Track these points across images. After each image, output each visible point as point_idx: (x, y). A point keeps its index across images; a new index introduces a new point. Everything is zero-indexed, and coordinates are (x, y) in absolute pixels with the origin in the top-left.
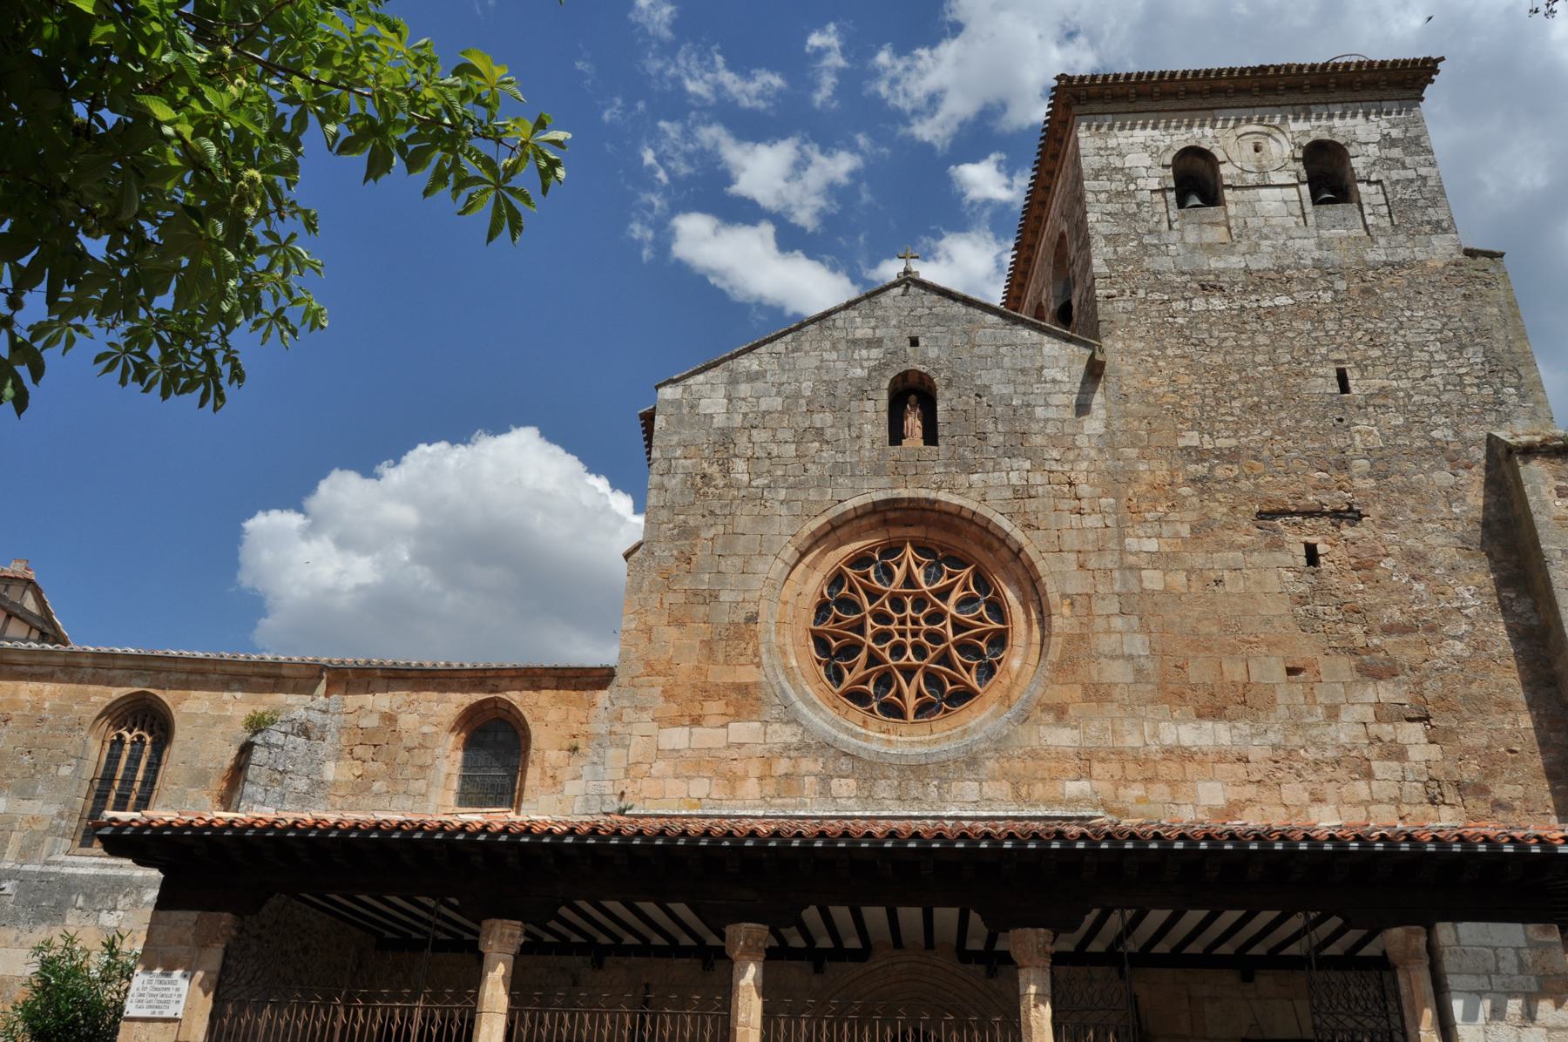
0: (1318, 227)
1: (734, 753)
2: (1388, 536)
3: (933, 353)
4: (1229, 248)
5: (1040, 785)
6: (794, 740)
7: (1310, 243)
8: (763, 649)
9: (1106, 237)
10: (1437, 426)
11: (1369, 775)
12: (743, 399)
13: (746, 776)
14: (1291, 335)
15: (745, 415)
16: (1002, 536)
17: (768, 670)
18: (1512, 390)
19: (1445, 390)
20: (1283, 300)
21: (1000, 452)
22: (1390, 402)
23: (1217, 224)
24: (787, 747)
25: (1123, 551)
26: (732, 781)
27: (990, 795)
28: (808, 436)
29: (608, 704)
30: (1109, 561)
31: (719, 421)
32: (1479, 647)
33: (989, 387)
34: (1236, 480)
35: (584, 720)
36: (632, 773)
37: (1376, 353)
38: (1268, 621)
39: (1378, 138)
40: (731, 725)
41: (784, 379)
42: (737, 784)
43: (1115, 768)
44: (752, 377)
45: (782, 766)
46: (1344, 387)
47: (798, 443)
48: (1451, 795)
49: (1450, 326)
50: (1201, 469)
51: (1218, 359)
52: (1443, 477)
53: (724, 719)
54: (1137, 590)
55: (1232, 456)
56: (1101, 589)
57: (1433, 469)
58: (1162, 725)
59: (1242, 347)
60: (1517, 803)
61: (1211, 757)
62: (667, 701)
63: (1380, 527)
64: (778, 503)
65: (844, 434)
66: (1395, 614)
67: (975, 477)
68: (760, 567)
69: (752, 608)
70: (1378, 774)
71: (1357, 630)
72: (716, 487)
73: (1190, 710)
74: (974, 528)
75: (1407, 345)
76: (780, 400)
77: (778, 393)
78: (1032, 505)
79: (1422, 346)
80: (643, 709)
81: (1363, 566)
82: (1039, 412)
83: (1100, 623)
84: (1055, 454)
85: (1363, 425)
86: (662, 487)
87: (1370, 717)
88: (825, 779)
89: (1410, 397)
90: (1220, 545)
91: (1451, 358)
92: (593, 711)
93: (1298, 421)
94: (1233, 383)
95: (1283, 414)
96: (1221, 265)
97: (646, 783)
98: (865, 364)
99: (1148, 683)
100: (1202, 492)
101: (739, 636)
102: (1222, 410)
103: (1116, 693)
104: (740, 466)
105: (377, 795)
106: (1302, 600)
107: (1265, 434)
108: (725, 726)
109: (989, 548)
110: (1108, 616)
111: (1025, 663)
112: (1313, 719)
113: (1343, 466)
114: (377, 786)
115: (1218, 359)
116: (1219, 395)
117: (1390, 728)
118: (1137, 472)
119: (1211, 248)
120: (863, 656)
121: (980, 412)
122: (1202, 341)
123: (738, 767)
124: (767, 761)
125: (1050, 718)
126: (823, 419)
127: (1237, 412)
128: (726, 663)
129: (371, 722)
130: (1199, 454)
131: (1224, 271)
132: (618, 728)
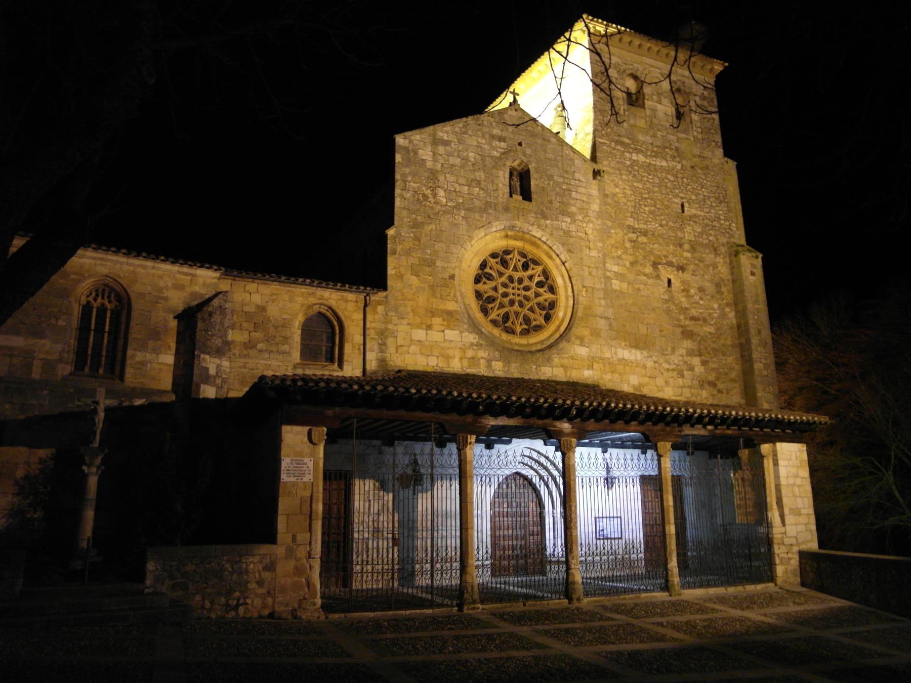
1: (447, 345)
3: (529, 152)
5: (574, 371)
6: (475, 341)
8: (458, 294)
9: (600, 110)
10: (711, 235)
11: (683, 376)
12: (441, 155)
13: (454, 357)
14: (666, 181)
15: (442, 165)
16: (558, 252)
17: (462, 305)
18: (734, 225)
19: (715, 220)
20: (664, 163)
21: (558, 211)
22: (697, 220)
23: (641, 117)
24: (472, 344)
25: (606, 270)
26: (448, 358)
27: (556, 373)
28: (474, 184)
29: (384, 313)
30: (601, 272)
31: (429, 164)
32: (718, 329)
33: (552, 176)
34: (646, 243)
35: (372, 320)
36: (400, 351)
37: (694, 197)
38: (654, 310)
40: (446, 331)
41: (461, 148)
42: (450, 360)
43: (601, 365)
44: (446, 143)
45: (470, 353)
46: (683, 211)
47: (469, 186)
48: (706, 386)
49: (718, 191)
50: (634, 236)
51: (640, 186)
52: (712, 256)
53: (442, 328)
54: (610, 289)
55: (645, 233)
56: (598, 286)
57: (710, 253)
58: (618, 349)
59: (648, 181)
60: (724, 391)
61: (634, 364)
62: (414, 315)
63: (692, 275)
64: (461, 218)
65: (490, 187)
66: (694, 312)
67: (548, 222)
68: (454, 250)
69: (452, 272)
70: (686, 376)
71: (682, 317)
72: (430, 202)
73: (627, 343)
74: (545, 247)
75: (704, 196)
76: (459, 160)
77: (458, 156)
78: (572, 240)
79: (709, 198)
80: (402, 318)
81: (686, 291)
82: (573, 194)
83: (596, 300)
84: (580, 218)
85: (689, 229)
86: (402, 196)
87: (685, 353)
88: (489, 362)
89: (703, 220)
90: (639, 273)
91: (717, 206)
92: (377, 316)
93: (667, 222)
94: (646, 199)
95: (663, 217)
96: (643, 139)
97: (407, 356)
98: (498, 150)
99: (613, 330)
100: (633, 247)
101: (447, 286)
102: (641, 210)
103: (603, 334)
104: (441, 193)
105: (261, 351)
106: (667, 301)
107: (657, 225)
108: (443, 331)
109: (551, 258)
110: (600, 298)
111: (565, 314)
112: (666, 353)
113: (681, 246)
114: (260, 346)
115: (640, 186)
116: (641, 203)
117: (690, 358)
118: (611, 233)
120: (498, 302)
121: (549, 189)
122: (635, 175)
123: (450, 352)
124: (463, 350)
125: (578, 342)
126: (480, 175)
127: (647, 213)
128: (441, 298)
129: (252, 309)
131: (644, 142)
132: (390, 326)
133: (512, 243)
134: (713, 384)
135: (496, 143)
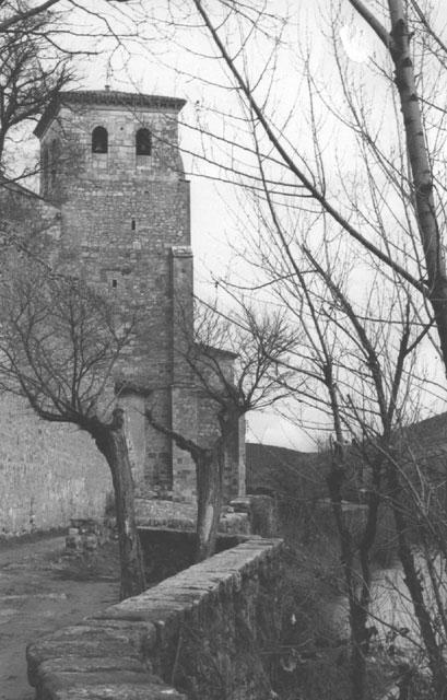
0: (137, 165)
2: (138, 279)
4: (107, 171)
7: (133, 172)
20: (120, 194)
37: (145, 216)
46: (134, 228)
55: (97, 250)
79: (159, 214)
113: (128, 255)
119: (100, 171)
130: (88, 249)
134: (147, 352)
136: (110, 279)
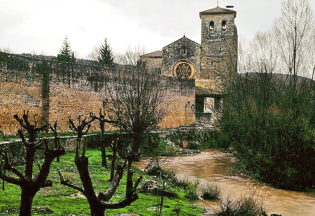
4: (213, 34)
39: (229, 20)
46: (221, 49)
55: (210, 56)
133: (183, 63)
135: (180, 45)
136: (214, 64)
